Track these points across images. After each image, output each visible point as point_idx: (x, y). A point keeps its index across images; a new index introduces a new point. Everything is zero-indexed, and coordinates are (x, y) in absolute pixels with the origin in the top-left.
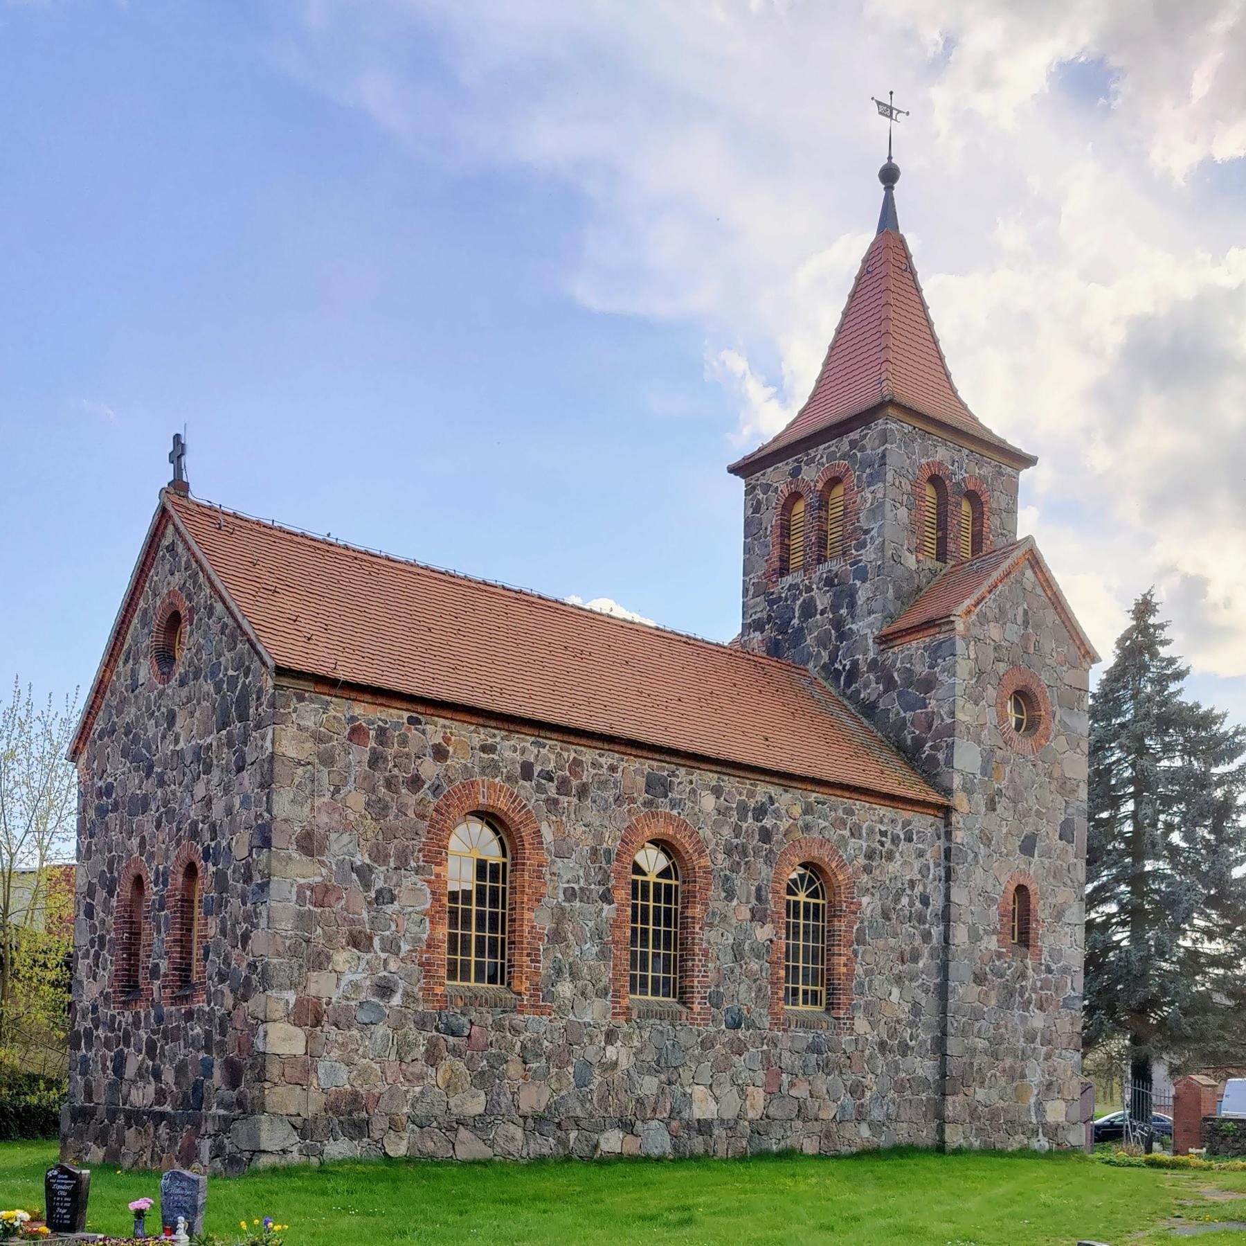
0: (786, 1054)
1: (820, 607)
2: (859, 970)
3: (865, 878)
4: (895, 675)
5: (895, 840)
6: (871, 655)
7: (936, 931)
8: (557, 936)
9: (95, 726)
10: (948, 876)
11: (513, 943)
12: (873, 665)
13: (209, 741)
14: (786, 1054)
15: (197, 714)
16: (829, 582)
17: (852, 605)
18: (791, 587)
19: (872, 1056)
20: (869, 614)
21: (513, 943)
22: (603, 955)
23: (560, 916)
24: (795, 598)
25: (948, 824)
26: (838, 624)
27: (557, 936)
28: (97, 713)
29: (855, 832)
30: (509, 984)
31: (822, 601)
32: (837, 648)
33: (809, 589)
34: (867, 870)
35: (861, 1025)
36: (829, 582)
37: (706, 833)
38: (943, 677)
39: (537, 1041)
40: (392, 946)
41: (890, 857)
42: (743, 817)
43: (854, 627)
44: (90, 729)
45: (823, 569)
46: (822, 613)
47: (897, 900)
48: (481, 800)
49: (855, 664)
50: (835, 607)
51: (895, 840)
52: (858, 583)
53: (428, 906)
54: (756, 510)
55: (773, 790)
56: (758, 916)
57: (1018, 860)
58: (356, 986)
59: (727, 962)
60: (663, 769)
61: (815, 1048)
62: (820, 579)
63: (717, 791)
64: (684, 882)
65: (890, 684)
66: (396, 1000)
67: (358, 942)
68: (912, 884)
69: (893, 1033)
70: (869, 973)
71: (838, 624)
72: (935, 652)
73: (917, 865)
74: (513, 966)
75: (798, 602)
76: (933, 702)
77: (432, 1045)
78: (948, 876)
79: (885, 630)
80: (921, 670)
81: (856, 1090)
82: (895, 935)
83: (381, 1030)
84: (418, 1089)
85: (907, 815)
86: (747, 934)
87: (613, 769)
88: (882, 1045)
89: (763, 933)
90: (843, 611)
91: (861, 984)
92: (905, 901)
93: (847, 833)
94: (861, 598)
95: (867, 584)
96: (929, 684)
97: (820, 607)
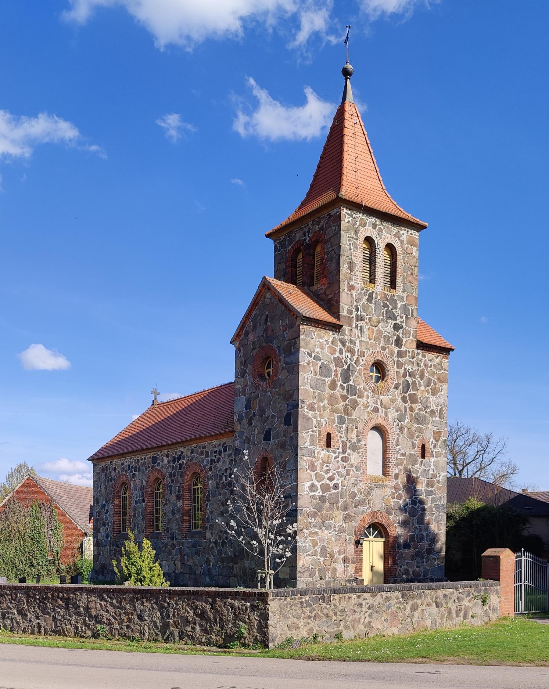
0: (186, 549)
2: (208, 512)
3: (210, 473)
5: (220, 452)
8: (134, 516)
14: (186, 549)
19: (212, 547)
22: (143, 520)
23: (135, 509)
27: (134, 516)
29: (207, 456)
34: (210, 469)
35: (208, 535)
37: (164, 471)
41: (219, 460)
42: (174, 463)
47: (221, 479)
51: (220, 452)
55: (182, 449)
56: (178, 498)
57: (262, 446)
59: (170, 515)
60: (155, 454)
61: (194, 546)
63: (167, 456)
67: (104, 525)
68: (226, 470)
69: (220, 538)
70: (211, 512)
73: (228, 461)
81: (208, 561)
82: (220, 494)
85: (224, 440)
86: (175, 505)
87: (145, 459)
88: (216, 543)
89: (179, 504)
91: (208, 518)
92: (224, 478)
93: (204, 456)
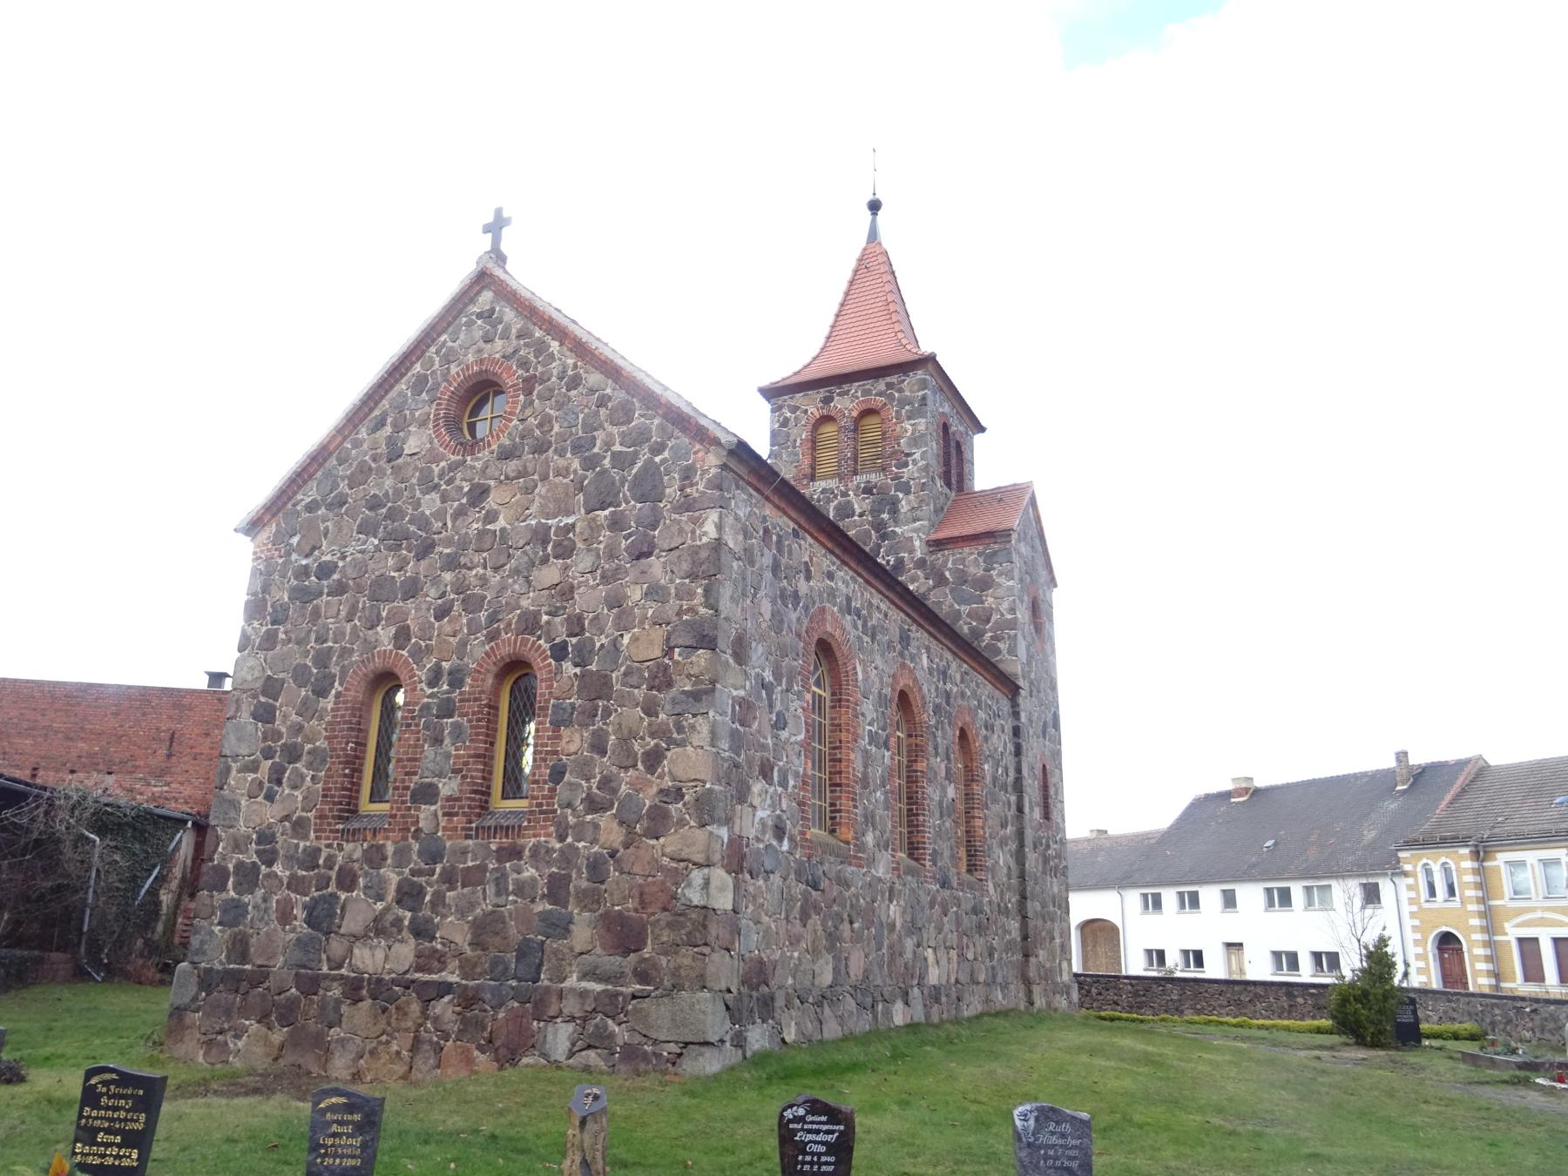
1: (858, 511)
4: (947, 574)
6: (919, 554)
7: (1013, 798)
9: (299, 497)
10: (1018, 752)
11: (839, 785)
12: (921, 564)
13: (570, 520)
15: (541, 489)
16: (868, 490)
17: (894, 511)
18: (824, 491)
20: (915, 521)
21: (839, 785)
24: (829, 501)
25: (1015, 705)
26: (879, 526)
28: (305, 482)
30: (833, 831)
31: (859, 504)
32: (879, 547)
33: (845, 494)
36: (868, 490)
38: (1002, 580)
39: (856, 896)
40: (783, 783)
43: (898, 530)
44: (290, 499)
45: (860, 479)
46: (861, 515)
48: (829, 629)
49: (900, 562)
50: (875, 512)
52: (901, 495)
53: (802, 737)
54: (785, 423)
58: (763, 822)
62: (858, 487)
64: (910, 736)
65: (941, 581)
66: (786, 846)
67: (766, 772)
71: (879, 526)
72: (990, 559)
74: (840, 811)
75: (832, 505)
76: (990, 600)
77: (806, 897)
78: (1018, 752)
79: (934, 537)
80: (976, 571)
83: (776, 879)
84: (796, 954)
90: (885, 516)
94: (904, 507)
95: (912, 497)
96: (985, 584)
97: (858, 511)
